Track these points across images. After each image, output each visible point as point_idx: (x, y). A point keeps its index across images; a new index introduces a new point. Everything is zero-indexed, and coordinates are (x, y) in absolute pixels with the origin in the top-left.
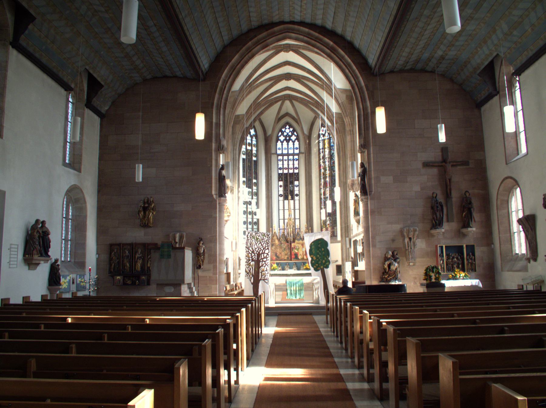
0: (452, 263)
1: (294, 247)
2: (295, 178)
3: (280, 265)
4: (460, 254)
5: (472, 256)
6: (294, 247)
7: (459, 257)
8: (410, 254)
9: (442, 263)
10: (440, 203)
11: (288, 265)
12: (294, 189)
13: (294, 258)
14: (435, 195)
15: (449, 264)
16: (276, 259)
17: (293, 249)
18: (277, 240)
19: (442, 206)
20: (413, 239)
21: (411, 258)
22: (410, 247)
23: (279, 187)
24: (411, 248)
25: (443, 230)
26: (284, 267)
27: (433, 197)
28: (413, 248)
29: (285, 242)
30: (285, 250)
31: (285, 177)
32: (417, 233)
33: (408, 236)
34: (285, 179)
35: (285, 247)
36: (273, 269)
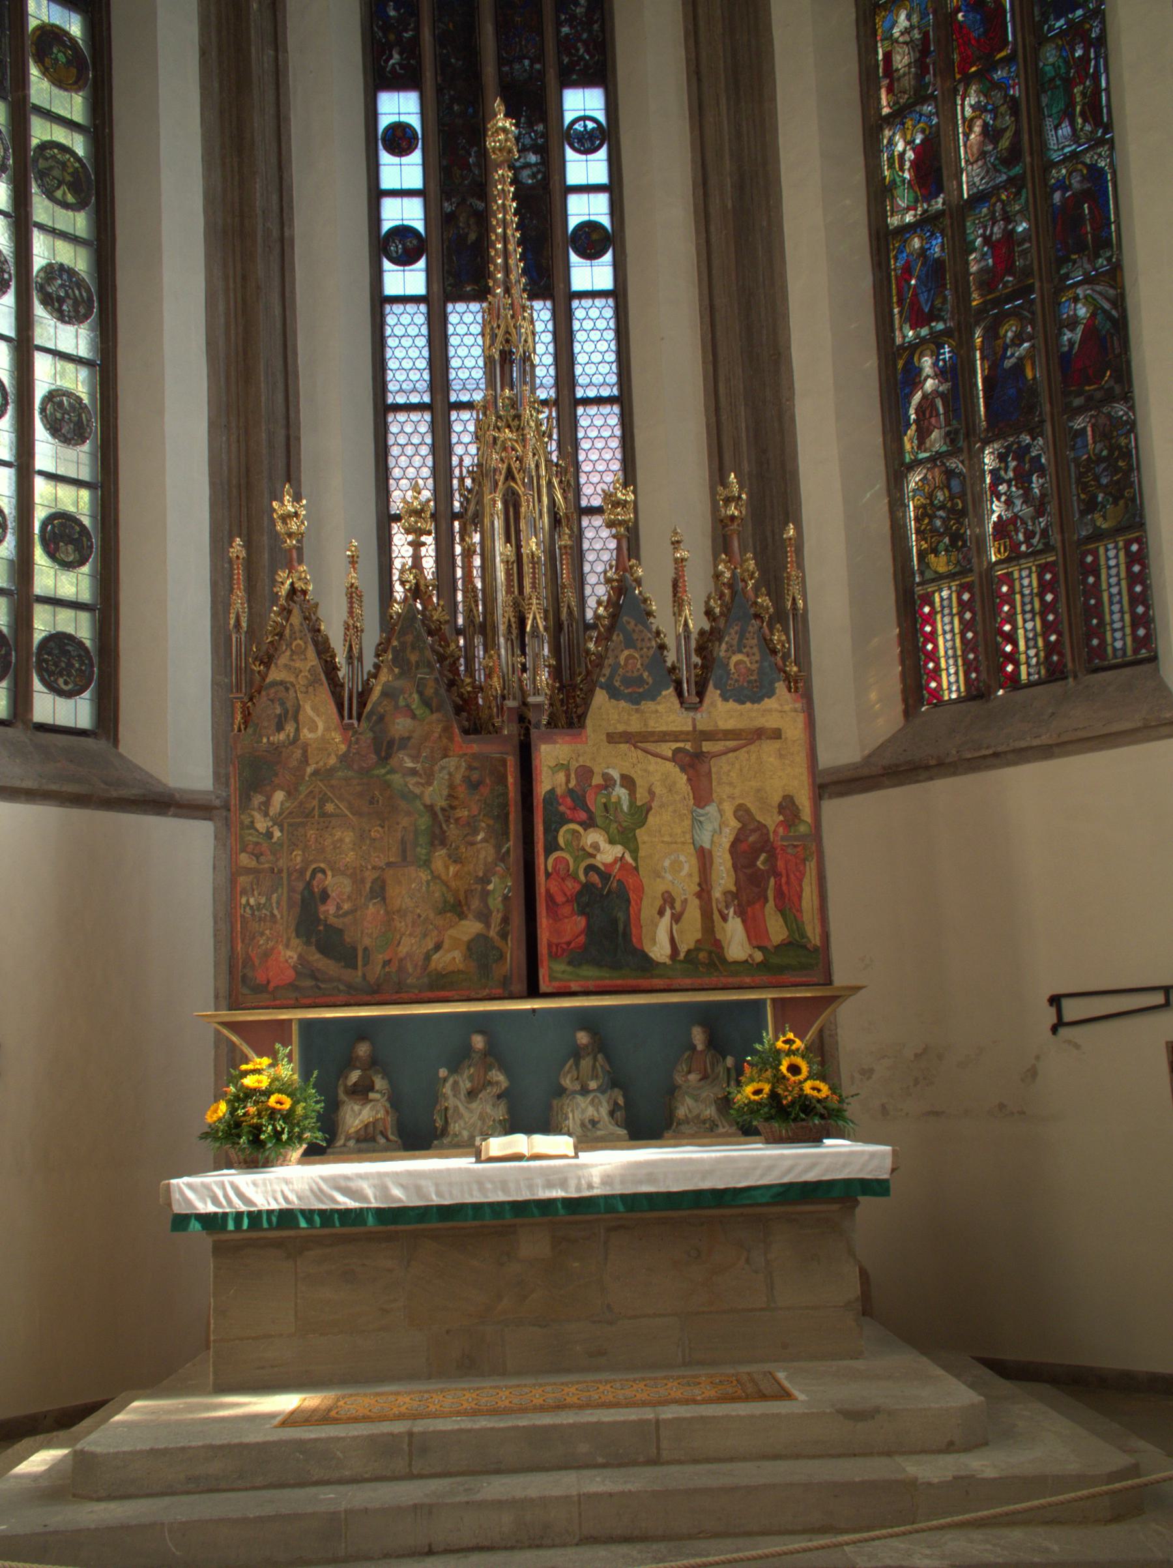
1: (578, 798)
2: (565, 45)
3: (373, 1063)
6: (578, 798)
11: (494, 1055)
12: (553, 167)
13: (578, 957)
16: (305, 970)
17: (555, 822)
18: (324, 694)
23: (385, 157)
26: (434, 1097)
29: (434, 723)
30: (438, 838)
31: (441, 40)
34: (443, 65)
35: (435, 794)
36: (233, 1128)
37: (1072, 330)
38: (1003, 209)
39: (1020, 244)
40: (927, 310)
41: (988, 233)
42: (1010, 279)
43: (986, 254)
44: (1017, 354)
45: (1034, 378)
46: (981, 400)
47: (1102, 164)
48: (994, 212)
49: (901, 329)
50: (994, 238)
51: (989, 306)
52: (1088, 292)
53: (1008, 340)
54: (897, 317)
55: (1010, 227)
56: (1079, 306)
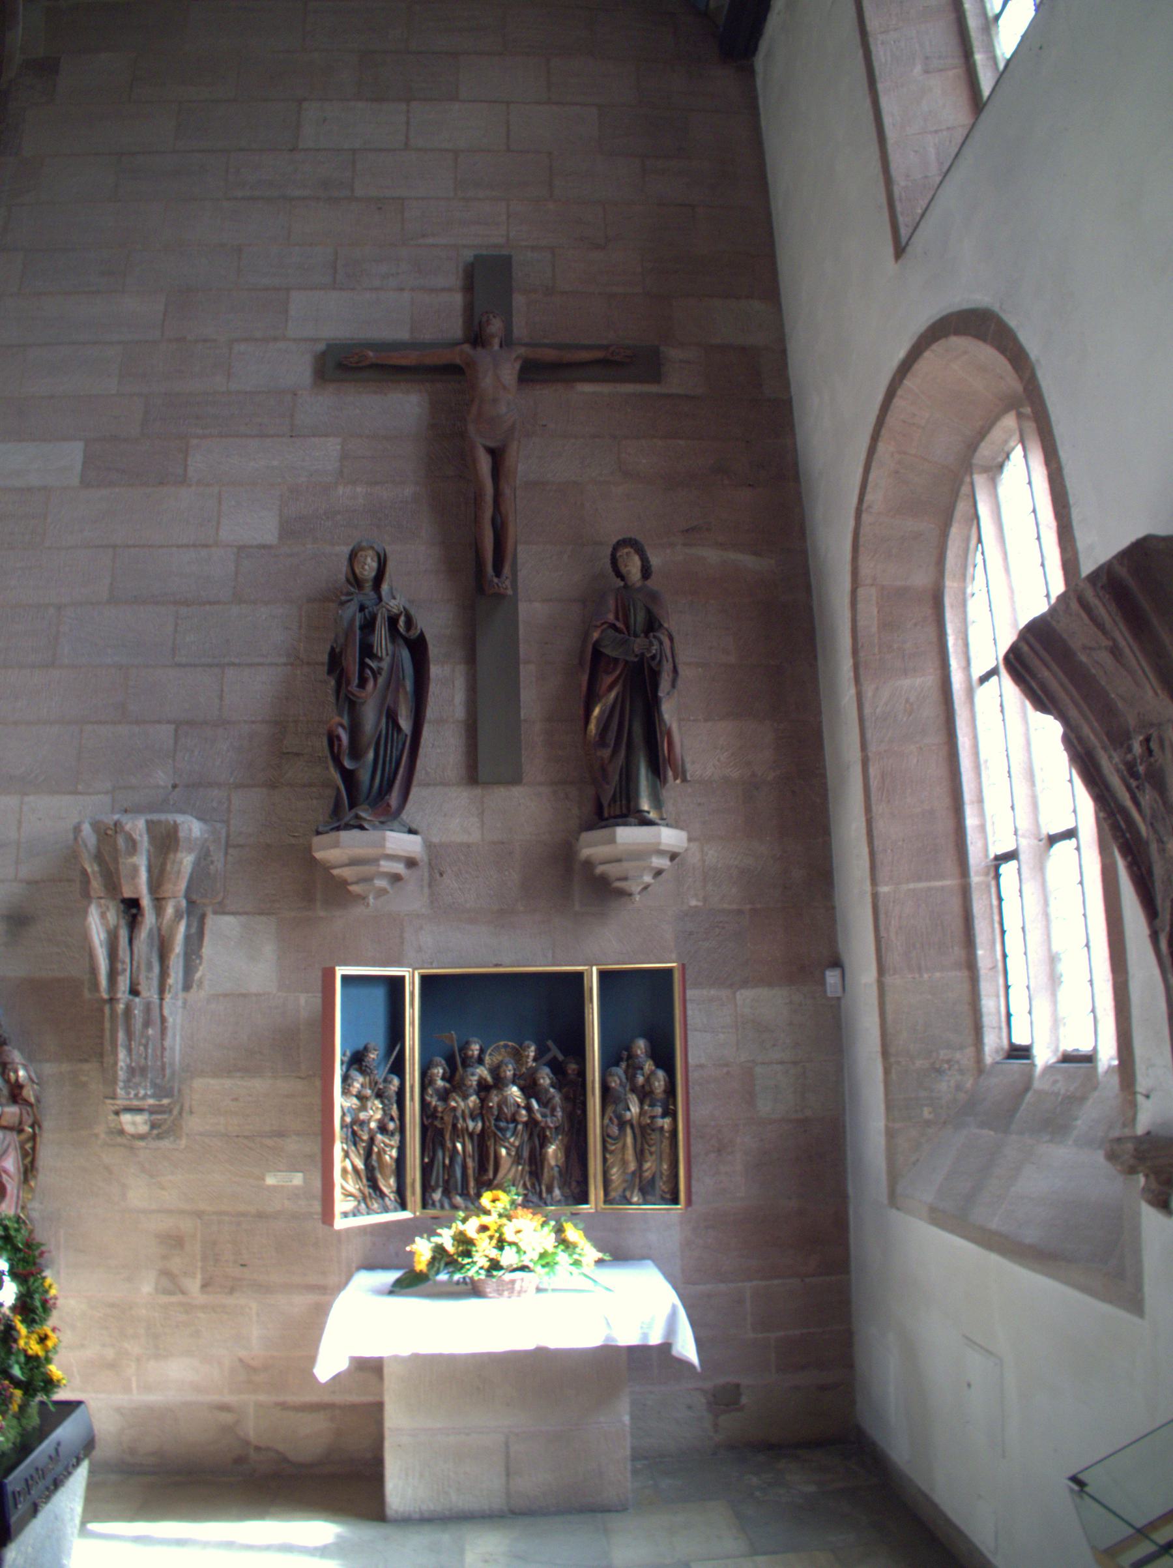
0: (475, 1126)
4: (555, 1052)
5: (649, 1066)
7: (545, 1078)
8: (121, 1036)
9: (383, 1129)
10: (393, 621)
14: (369, 566)
15: (457, 1133)
19: (418, 648)
20: (159, 909)
21: (131, 1071)
22: (123, 983)
24: (134, 992)
25: (399, 842)
27: (355, 581)
28: (149, 991)
32: (186, 861)
33: (112, 884)
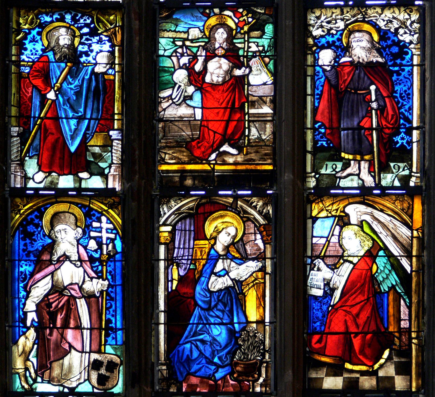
37: (333, 267)
38: (230, 38)
39: (252, 104)
40: (73, 149)
41: (198, 67)
42: (234, 151)
43: (191, 98)
44: (233, 275)
45: (261, 322)
46: (162, 328)
47: (407, 38)
48: (211, 39)
49: (22, 164)
50: (208, 79)
51: (189, 182)
52: (368, 218)
53: (219, 247)
54: (16, 141)
55: (238, 72)
56: (348, 232)
